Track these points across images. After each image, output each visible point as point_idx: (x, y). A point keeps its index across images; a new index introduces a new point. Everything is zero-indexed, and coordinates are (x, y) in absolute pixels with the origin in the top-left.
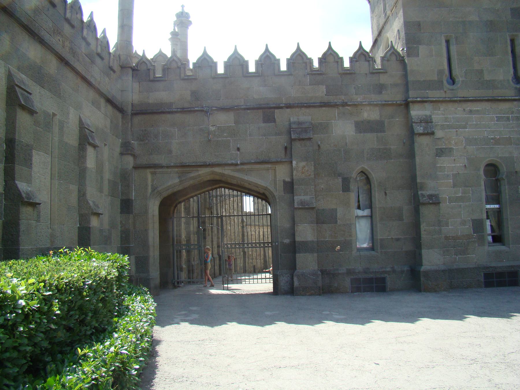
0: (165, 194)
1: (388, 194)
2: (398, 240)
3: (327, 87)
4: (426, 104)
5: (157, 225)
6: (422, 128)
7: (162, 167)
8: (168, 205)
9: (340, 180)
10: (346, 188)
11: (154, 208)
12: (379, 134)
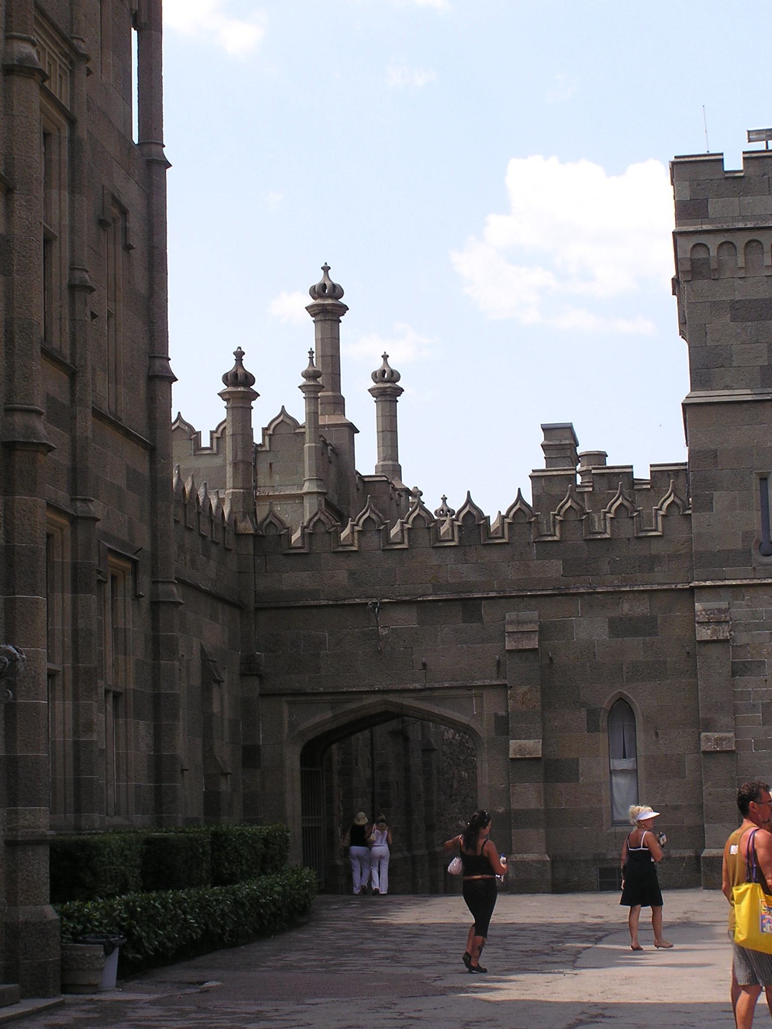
0: (310, 736)
1: (660, 736)
2: (676, 808)
3: (565, 562)
4: (721, 590)
5: (298, 785)
6: (709, 632)
7: (306, 694)
8: (315, 752)
9: (584, 712)
10: (593, 727)
11: (293, 759)
12: (647, 639)
